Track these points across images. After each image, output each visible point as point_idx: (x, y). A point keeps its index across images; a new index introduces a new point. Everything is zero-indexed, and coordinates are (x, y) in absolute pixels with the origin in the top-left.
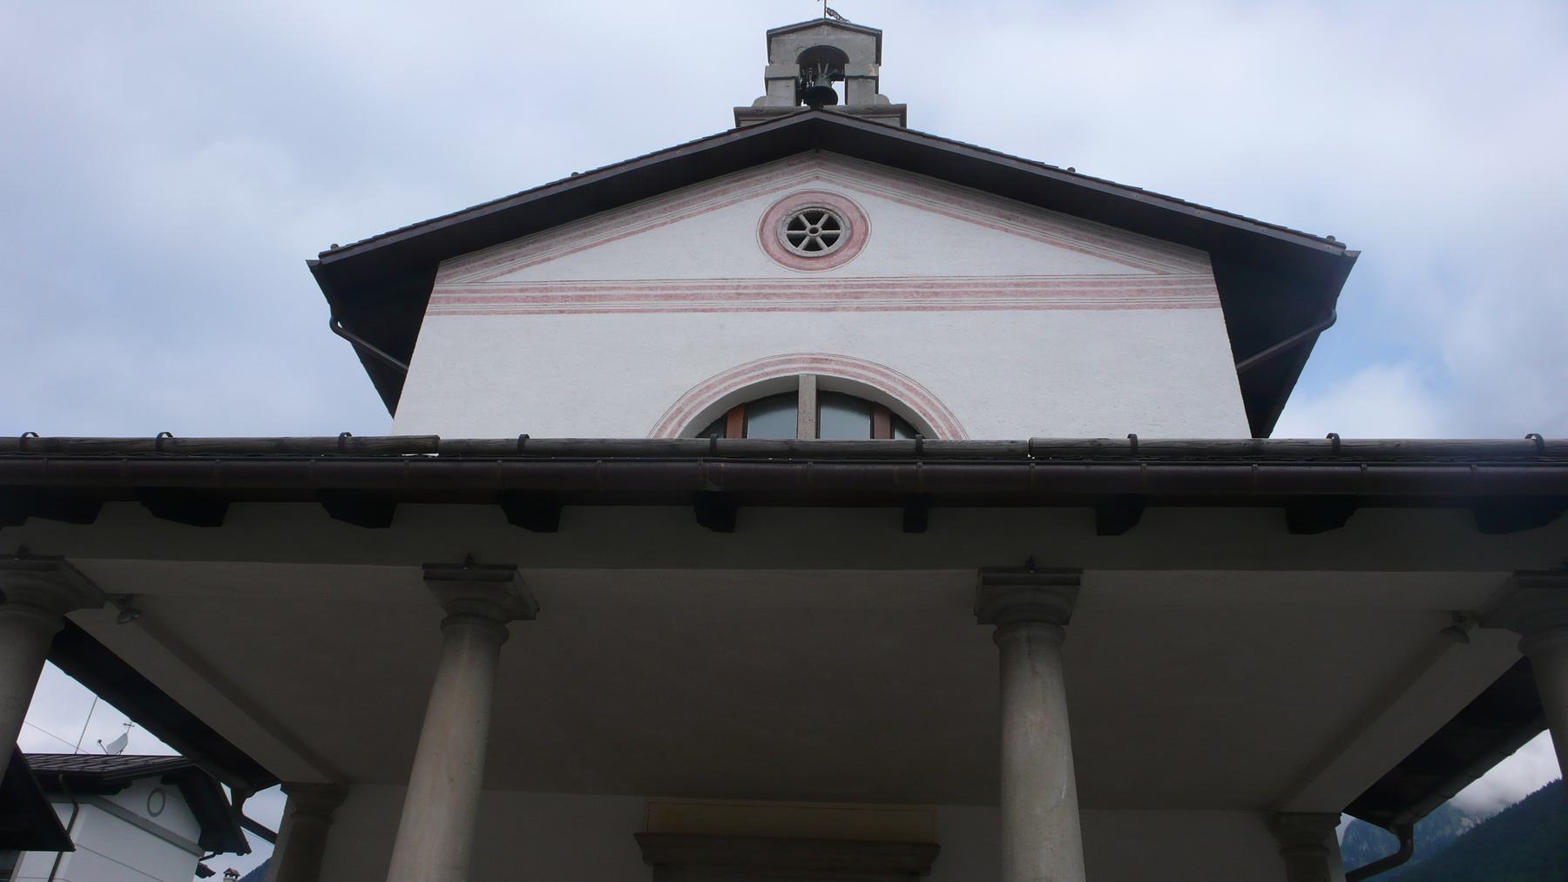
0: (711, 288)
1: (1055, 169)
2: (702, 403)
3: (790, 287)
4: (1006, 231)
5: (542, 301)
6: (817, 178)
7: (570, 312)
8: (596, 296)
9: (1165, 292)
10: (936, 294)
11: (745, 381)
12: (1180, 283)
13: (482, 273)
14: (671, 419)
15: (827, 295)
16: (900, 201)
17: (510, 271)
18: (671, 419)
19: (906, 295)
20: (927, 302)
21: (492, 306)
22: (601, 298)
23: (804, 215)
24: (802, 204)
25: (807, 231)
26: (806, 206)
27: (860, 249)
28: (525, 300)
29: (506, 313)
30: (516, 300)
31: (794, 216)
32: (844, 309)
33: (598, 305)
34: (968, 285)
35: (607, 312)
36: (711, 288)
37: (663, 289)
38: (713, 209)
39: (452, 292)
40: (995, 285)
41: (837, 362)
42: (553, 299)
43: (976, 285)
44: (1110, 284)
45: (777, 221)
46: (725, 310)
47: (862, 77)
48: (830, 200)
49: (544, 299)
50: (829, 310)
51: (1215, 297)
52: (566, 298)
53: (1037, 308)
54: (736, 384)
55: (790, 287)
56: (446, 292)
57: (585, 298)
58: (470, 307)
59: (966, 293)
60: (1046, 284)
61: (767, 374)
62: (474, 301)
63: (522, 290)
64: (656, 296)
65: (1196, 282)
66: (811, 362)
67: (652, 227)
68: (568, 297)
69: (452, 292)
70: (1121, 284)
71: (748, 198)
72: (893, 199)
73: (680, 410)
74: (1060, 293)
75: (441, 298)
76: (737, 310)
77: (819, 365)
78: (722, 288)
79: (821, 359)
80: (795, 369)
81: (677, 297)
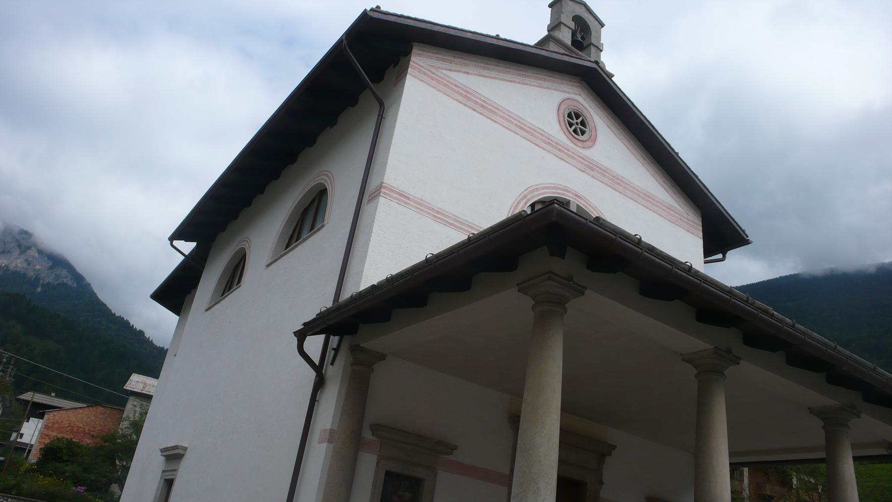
0: (539, 133)
1: (673, 150)
2: (534, 196)
3: (568, 150)
4: (643, 165)
5: (465, 98)
6: (580, 95)
7: (478, 113)
8: (490, 109)
9: (688, 223)
10: (619, 184)
11: (551, 193)
12: (692, 221)
13: (439, 64)
14: (522, 199)
15: (580, 162)
16: (609, 127)
17: (450, 70)
18: (522, 199)
19: (610, 179)
20: (616, 186)
21: (441, 87)
22: (492, 111)
23: (574, 113)
24: (574, 106)
25: (575, 121)
26: (575, 108)
27: (594, 144)
28: (457, 92)
29: (449, 96)
30: (453, 90)
31: (570, 110)
32: (587, 173)
33: (490, 115)
34: (629, 185)
35: (495, 122)
36: (539, 133)
37: (519, 122)
38: (540, 87)
39: (421, 66)
40: (638, 191)
41: (584, 201)
42: (469, 99)
43: (632, 187)
44: (673, 211)
45: (565, 110)
46: (544, 149)
47: (597, 47)
48: (584, 110)
49: (467, 97)
50: (582, 171)
51: (701, 234)
52: (476, 103)
53: (650, 210)
54: (548, 193)
55: (568, 150)
56: (418, 64)
57: (485, 108)
58: (430, 81)
59: (629, 190)
60: (653, 199)
61: (559, 194)
62: (433, 79)
63: (456, 86)
64: (516, 124)
65: (695, 223)
66: (575, 196)
67: (514, 82)
68: (477, 102)
69: (418, 64)
70: (676, 212)
71: (554, 89)
72: (606, 124)
73: (525, 196)
74: (657, 206)
75: (415, 67)
76: (548, 151)
77: (577, 199)
78: (542, 134)
79: (579, 196)
80: (569, 197)
81: (525, 130)
